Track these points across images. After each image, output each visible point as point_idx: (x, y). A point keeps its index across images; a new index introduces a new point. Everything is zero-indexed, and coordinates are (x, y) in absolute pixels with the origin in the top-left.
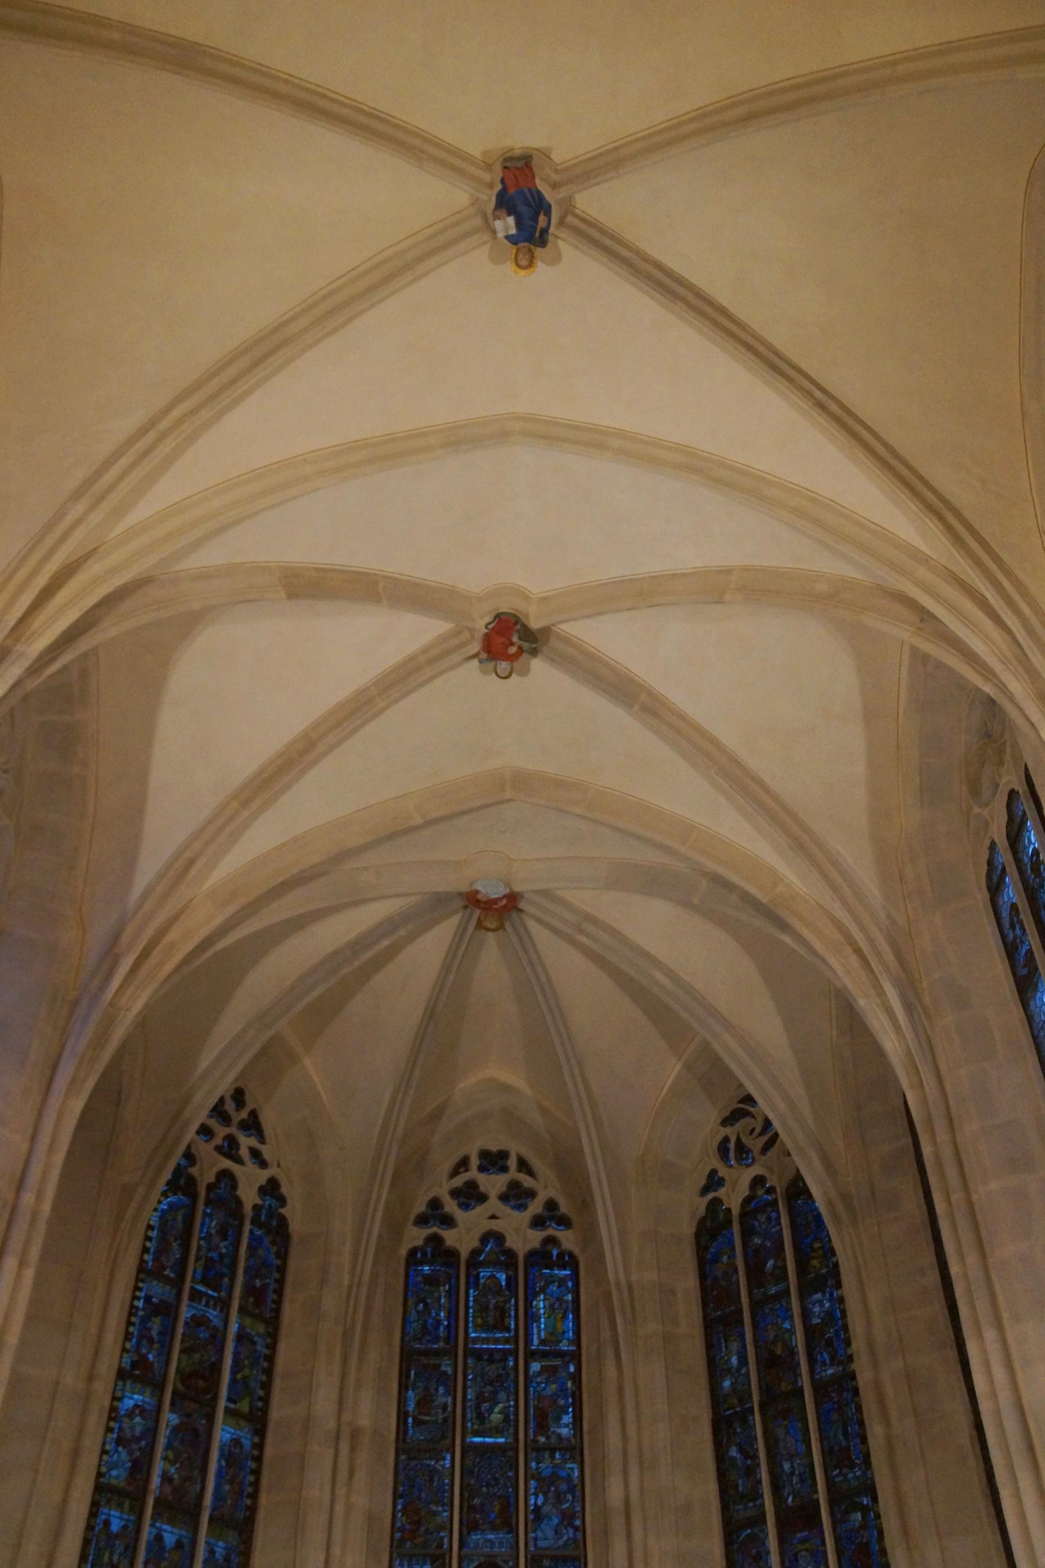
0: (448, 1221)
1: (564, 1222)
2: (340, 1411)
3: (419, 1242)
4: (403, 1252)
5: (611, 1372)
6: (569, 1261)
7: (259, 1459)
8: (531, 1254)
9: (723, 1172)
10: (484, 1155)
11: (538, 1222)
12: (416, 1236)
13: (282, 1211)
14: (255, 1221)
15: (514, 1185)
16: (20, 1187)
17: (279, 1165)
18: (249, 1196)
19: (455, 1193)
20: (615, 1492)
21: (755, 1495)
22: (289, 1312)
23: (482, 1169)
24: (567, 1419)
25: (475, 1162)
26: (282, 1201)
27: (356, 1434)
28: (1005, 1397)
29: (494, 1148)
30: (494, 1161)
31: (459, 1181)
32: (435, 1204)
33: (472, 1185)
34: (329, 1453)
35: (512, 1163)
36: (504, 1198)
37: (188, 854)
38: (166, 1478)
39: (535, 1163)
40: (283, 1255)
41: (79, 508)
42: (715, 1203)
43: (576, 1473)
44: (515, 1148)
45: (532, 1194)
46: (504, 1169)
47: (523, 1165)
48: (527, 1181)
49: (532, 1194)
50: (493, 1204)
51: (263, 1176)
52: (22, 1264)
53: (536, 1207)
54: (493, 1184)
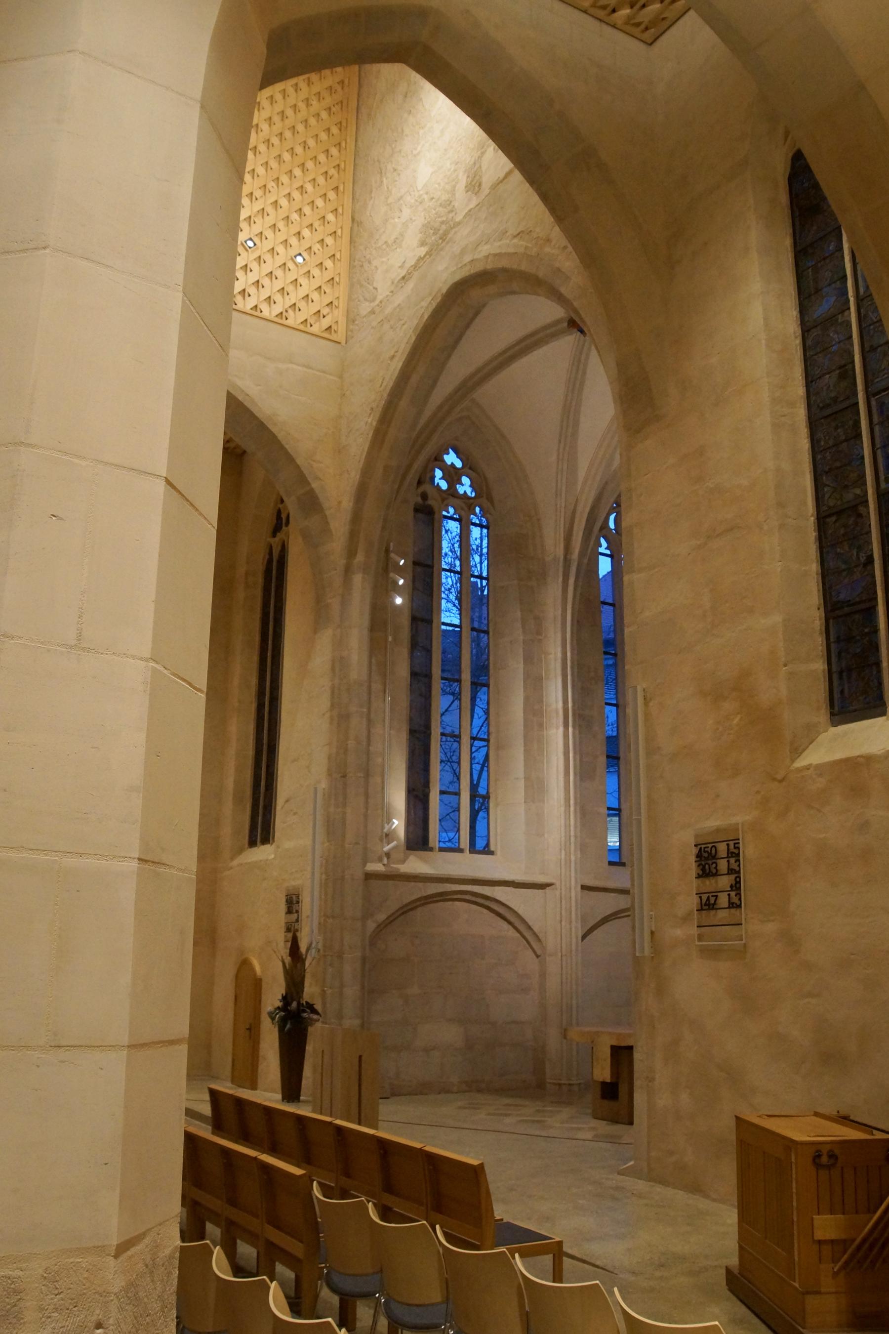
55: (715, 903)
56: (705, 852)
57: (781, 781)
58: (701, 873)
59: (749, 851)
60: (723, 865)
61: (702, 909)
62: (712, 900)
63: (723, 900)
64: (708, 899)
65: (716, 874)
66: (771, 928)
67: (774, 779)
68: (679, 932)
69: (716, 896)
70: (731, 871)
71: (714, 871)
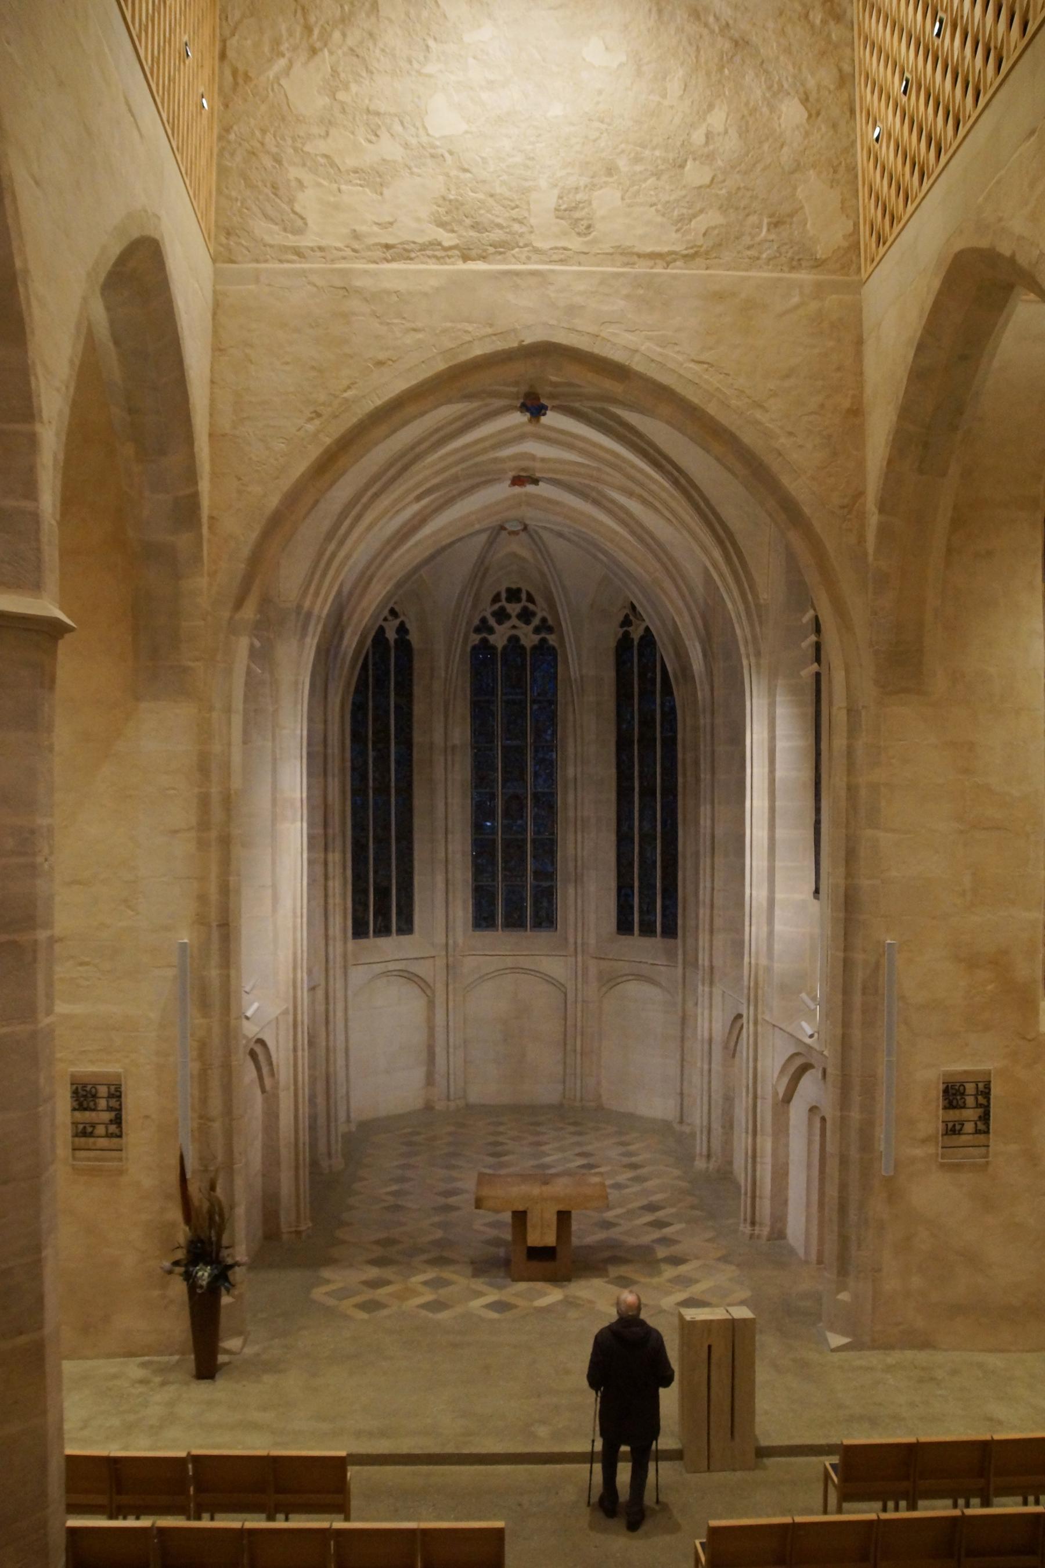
0: (491, 631)
1: (550, 630)
2: (446, 740)
3: (477, 642)
4: (469, 649)
5: (571, 717)
6: (552, 651)
7: (411, 761)
8: (534, 648)
9: (631, 617)
10: (509, 590)
11: (537, 630)
12: (475, 639)
13: (408, 637)
14: (397, 648)
15: (525, 609)
16: (325, 746)
17: (404, 614)
18: (391, 635)
19: (494, 614)
20: (571, 772)
21: (632, 779)
22: (417, 690)
23: (509, 600)
24: (549, 732)
25: (504, 595)
26: (407, 632)
27: (454, 747)
28: (708, 831)
29: (514, 586)
30: (514, 595)
31: (496, 606)
32: (484, 620)
33: (502, 609)
34: (442, 759)
35: (524, 596)
36: (519, 617)
37: (369, 573)
38: (374, 779)
39: (538, 598)
40: (410, 660)
41: (332, 547)
42: (626, 636)
43: (555, 757)
44: (525, 587)
45: (533, 614)
46: (519, 600)
47: (530, 599)
48: (531, 606)
49: (533, 614)
50: (514, 621)
51: (397, 622)
52: (333, 776)
53: (536, 621)
54: (514, 609)
55: (961, 1130)
56: (952, 1089)
57: (1030, 1041)
58: (947, 1105)
59: (996, 1090)
60: (970, 1101)
61: (946, 1134)
62: (958, 1127)
63: (969, 1127)
64: (954, 1126)
65: (964, 1107)
66: (1013, 1148)
67: (1024, 1038)
68: (918, 1152)
69: (963, 1125)
70: (979, 1105)
71: (961, 1103)
